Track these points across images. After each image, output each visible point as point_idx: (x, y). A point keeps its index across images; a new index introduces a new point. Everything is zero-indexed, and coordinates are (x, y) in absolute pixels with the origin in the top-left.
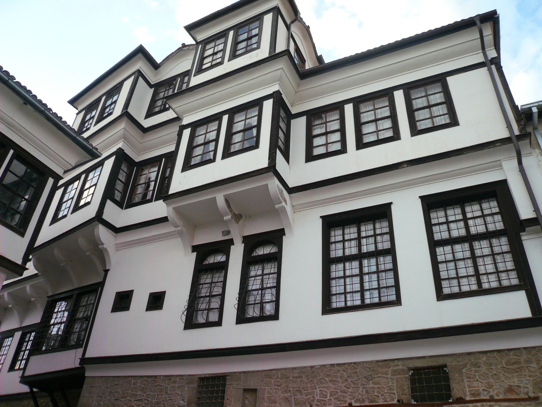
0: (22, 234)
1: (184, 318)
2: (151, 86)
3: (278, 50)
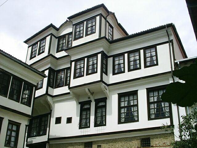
0: (30, 107)
1: (79, 125)
2: (56, 38)
3: (102, 36)
